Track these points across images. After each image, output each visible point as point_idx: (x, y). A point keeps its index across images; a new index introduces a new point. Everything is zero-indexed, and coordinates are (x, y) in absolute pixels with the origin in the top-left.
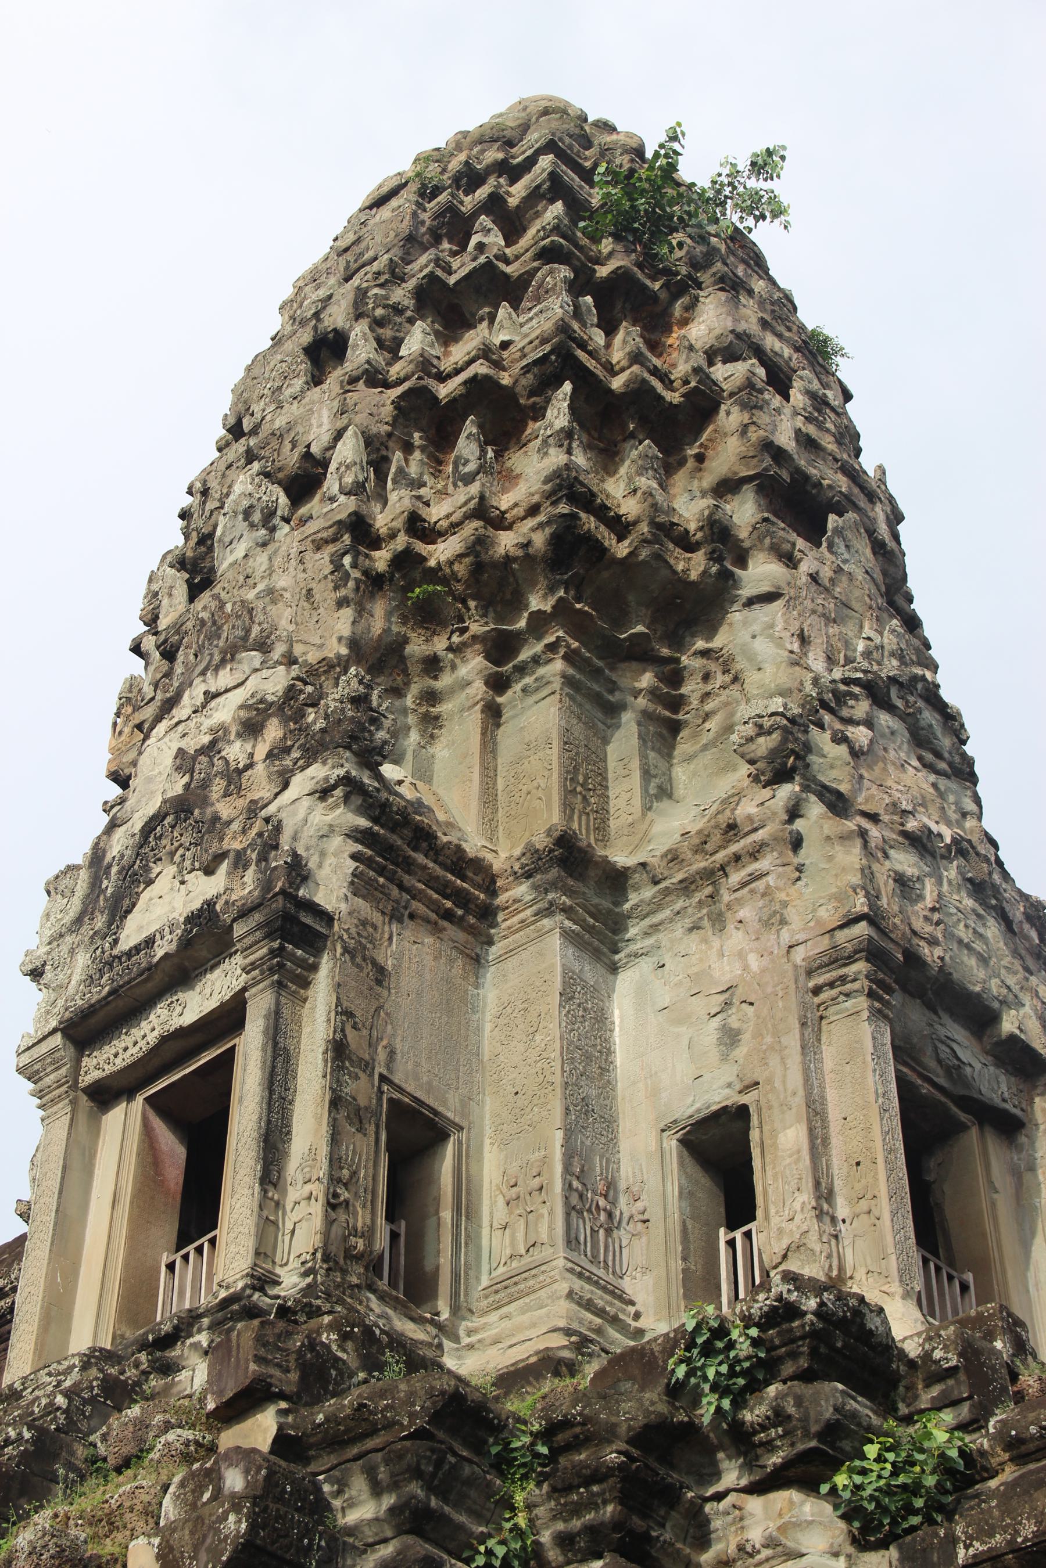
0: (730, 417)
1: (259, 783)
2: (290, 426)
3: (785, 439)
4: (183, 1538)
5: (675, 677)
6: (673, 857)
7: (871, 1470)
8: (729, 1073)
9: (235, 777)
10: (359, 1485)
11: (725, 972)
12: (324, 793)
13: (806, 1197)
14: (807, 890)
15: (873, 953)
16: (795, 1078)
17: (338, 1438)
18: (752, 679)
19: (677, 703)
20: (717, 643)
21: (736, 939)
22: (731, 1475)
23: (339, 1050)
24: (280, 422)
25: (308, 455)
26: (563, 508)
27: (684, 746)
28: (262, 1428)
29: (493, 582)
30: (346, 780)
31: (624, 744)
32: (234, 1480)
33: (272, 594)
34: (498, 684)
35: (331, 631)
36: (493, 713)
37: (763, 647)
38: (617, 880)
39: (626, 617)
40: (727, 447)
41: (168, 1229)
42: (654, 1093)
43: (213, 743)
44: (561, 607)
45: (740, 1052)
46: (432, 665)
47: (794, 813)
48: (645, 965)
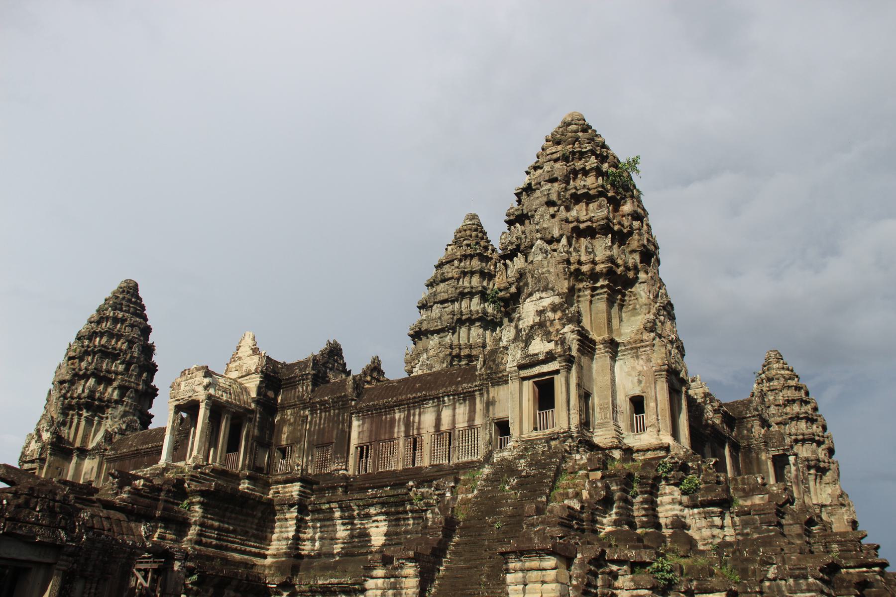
0: (636, 237)
2: (548, 228)
3: (645, 242)
4: (593, 492)
5: (624, 295)
6: (629, 343)
7: (685, 485)
8: (640, 389)
9: (552, 322)
10: (614, 484)
11: (639, 368)
12: (573, 332)
13: (655, 416)
14: (655, 355)
15: (667, 371)
16: (653, 394)
17: (610, 476)
18: (640, 300)
19: (624, 301)
20: (633, 290)
21: (641, 362)
22: (663, 483)
23: (579, 385)
24: (545, 225)
25: (552, 237)
26: (610, 265)
27: (624, 310)
28: (599, 474)
29: (594, 276)
30: (578, 331)
31: (615, 310)
32: (599, 484)
33: (549, 272)
34: (592, 296)
35: (564, 286)
36: (591, 302)
37: (642, 293)
38: (617, 344)
39: (618, 285)
40: (634, 242)
41: (537, 406)
42: (624, 388)
44: (607, 286)
45: (642, 385)
46: (580, 290)
47: (654, 339)
48: (622, 362)
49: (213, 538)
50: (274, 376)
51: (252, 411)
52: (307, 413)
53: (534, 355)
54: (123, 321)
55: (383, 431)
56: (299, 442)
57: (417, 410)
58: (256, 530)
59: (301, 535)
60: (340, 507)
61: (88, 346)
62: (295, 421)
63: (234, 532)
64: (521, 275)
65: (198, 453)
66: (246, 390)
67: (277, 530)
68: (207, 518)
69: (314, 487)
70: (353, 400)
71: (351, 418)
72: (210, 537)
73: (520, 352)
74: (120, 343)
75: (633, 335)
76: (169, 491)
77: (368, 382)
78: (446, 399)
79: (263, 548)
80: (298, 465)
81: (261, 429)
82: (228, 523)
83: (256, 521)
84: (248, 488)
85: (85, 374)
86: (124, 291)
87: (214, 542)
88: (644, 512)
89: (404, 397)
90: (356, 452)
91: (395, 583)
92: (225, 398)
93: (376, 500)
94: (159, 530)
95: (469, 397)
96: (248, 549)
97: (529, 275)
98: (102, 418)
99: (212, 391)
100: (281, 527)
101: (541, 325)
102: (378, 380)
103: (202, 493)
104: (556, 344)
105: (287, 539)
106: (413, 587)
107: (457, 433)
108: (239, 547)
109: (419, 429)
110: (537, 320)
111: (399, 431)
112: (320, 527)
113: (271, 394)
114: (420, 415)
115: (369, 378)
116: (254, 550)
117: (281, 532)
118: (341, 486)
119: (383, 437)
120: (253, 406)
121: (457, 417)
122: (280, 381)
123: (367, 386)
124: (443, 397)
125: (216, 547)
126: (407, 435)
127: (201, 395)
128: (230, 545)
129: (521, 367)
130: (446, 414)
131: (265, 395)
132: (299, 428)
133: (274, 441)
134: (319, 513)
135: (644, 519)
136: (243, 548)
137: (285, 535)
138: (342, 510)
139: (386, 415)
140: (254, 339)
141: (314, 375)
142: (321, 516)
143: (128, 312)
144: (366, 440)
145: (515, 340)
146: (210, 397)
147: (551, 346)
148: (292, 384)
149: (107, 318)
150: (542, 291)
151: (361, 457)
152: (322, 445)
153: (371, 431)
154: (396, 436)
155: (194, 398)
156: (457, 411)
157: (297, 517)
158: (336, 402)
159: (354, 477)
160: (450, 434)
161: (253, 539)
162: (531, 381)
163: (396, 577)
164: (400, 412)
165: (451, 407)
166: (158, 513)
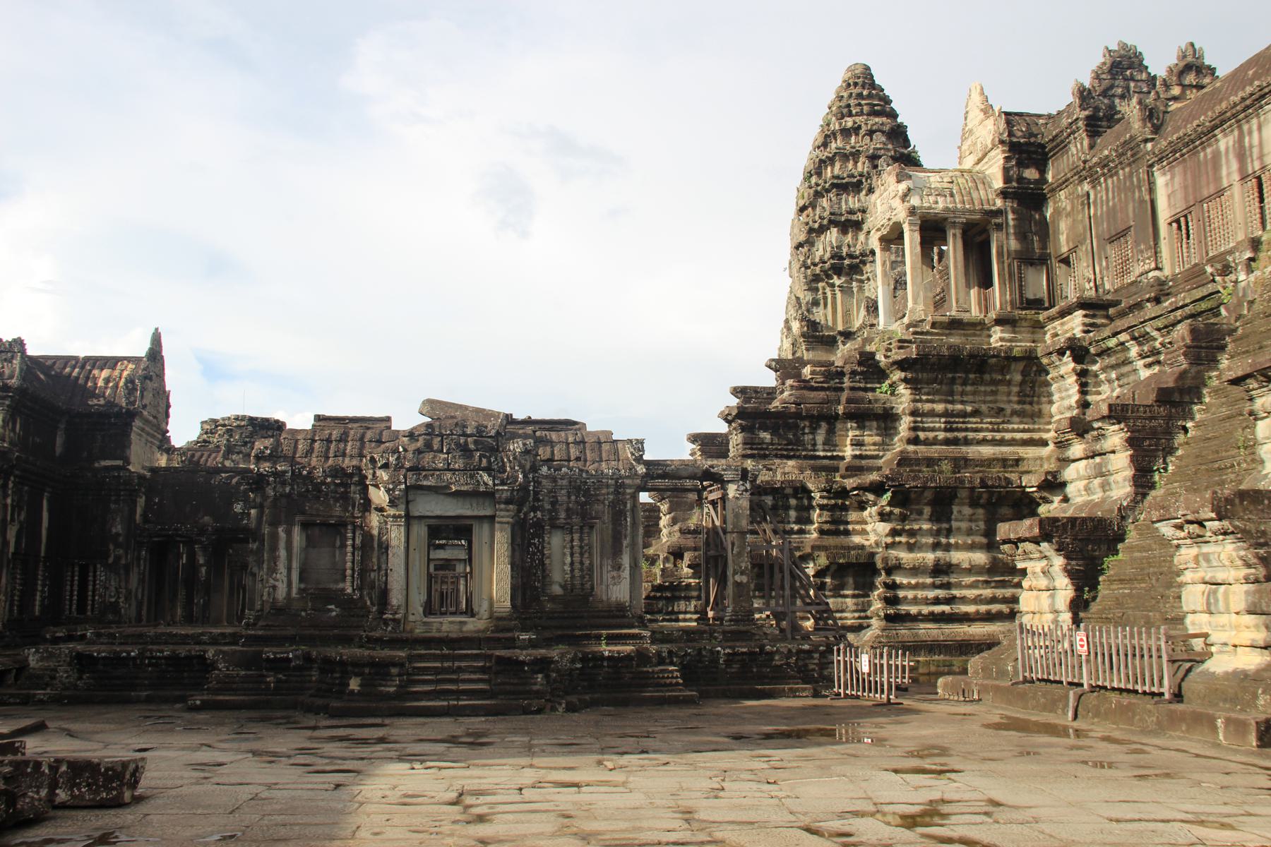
49: (939, 429)
50: (1027, 146)
51: (999, 213)
52: (1086, 187)
54: (856, 129)
55: (1204, 182)
56: (1082, 242)
57: (1254, 122)
58: (1019, 402)
59: (1089, 398)
60: (1134, 338)
61: (817, 185)
62: (1073, 208)
63: (976, 413)
65: (915, 302)
66: (985, 182)
67: (1055, 398)
68: (920, 401)
69: (1111, 311)
70: (1146, 141)
71: (1150, 175)
72: (933, 430)
74: (859, 164)
76: (854, 373)
77: (1175, 99)
79: (1039, 430)
80: (1089, 281)
81: (1022, 236)
82: (962, 402)
83: (1015, 389)
84: (1002, 339)
85: (821, 226)
86: (849, 85)
87: (941, 435)
89: (1224, 105)
90: (1170, 233)
91: (1100, 465)
92: (941, 206)
93: (1179, 313)
94: (851, 434)
96: (1008, 436)
98: (862, 281)
99: (915, 201)
100: (1060, 390)
102: (1200, 87)
103: (902, 365)
105: (1070, 408)
106: (1124, 469)
108: (989, 435)
109: (1261, 157)
111: (1230, 172)
112: (1118, 379)
113: (1031, 174)
114: (1260, 128)
115: (1176, 91)
116: (1018, 436)
117: (1062, 399)
118: (1148, 300)
119: (1206, 194)
120: (999, 203)
122: (1043, 146)
123: (1174, 106)
125: (947, 442)
126: (1244, 178)
127: (901, 214)
128: (971, 435)
131: (1020, 179)
132: (1080, 217)
133: (1051, 250)
134: (1109, 356)
136: (998, 436)
137: (1066, 403)
138: (1140, 344)
139: (1204, 149)
140: (982, 93)
141: (1087, 118)
142: (1112, 360)
143: (861, 113)
144: (1180, 206)
146: (912, 211)
148: (1060, 145)
149: (834, 133)
152: (1117, 237)
153: (1186, 187)
154: (1225, 183)
155: (894, 219)
157: (1074, 370)
158: (1123, 154)
159: (1175, 275)
161: (1016, 419)
164: (1226, 135)
166: (841, 409)
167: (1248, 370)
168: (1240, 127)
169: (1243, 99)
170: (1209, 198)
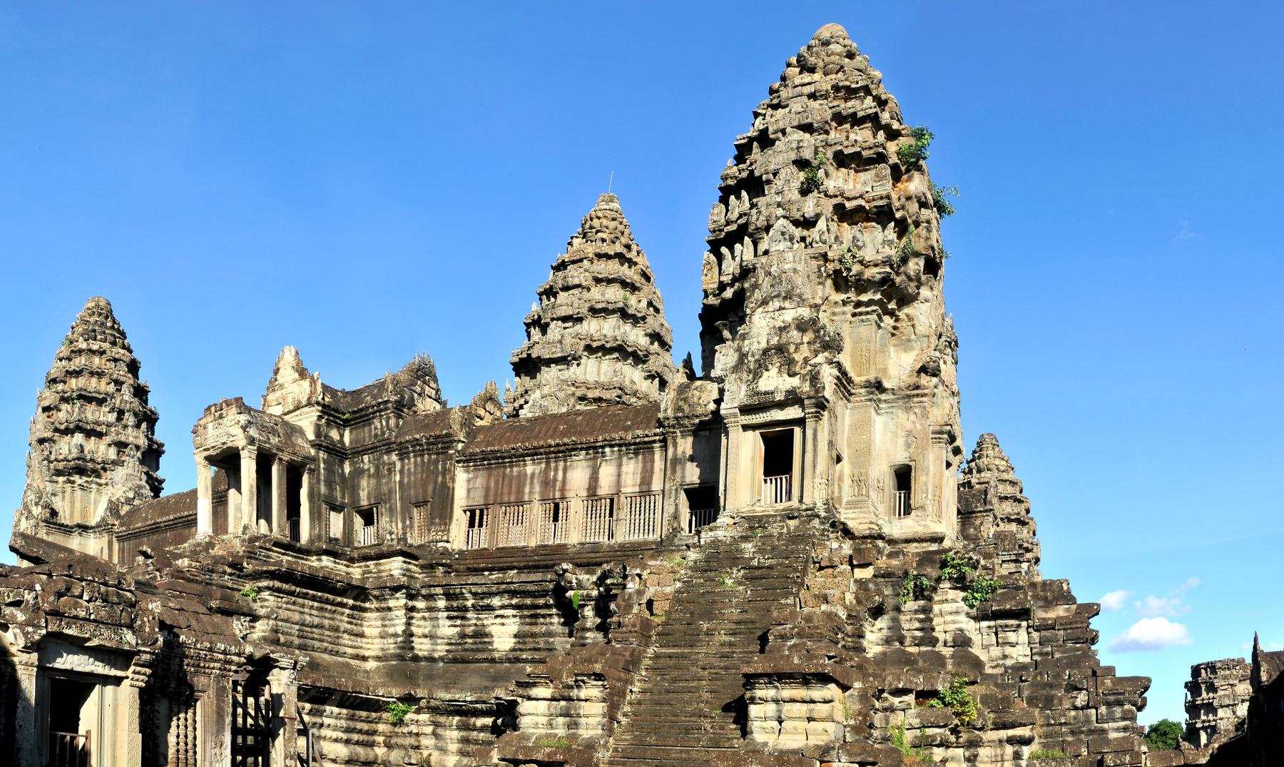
1: (805, 351)
11: (909, 426)
23: (831, 444)
43: (785, 328)
45: (911, 450)
53: (766, 393)
57: (561, 464)
64: (746, 272)
73: (744, 387)
75: (904, 377)
78: (607, 450)
88: (917, 625)
95: (642, 448)
97: (761, 273)
101: (781, 349)
104: (803, 379)
107: (622, 498)
109: (563, 490)
110: (775, 341)
111: (533, 491)
119: (506, 499)
121: (623, 477)
124: (603, 447)
129: (745, 410)
130: (607, 473)
135: (918, 634)
139: (511, 467)
144: (478, 500)
145: (736, 368)
147: (795, 382)
150: (785, 298)
151: (471, 525)
154: (526, 498)
156: (624, 468)
160: (612, 500)
162: (757, 432)
163: (569, 699)
165: (614, 463)
167: (769, 671)
168: (548, 463)
169: (558, 445)
170: (509, 504)
